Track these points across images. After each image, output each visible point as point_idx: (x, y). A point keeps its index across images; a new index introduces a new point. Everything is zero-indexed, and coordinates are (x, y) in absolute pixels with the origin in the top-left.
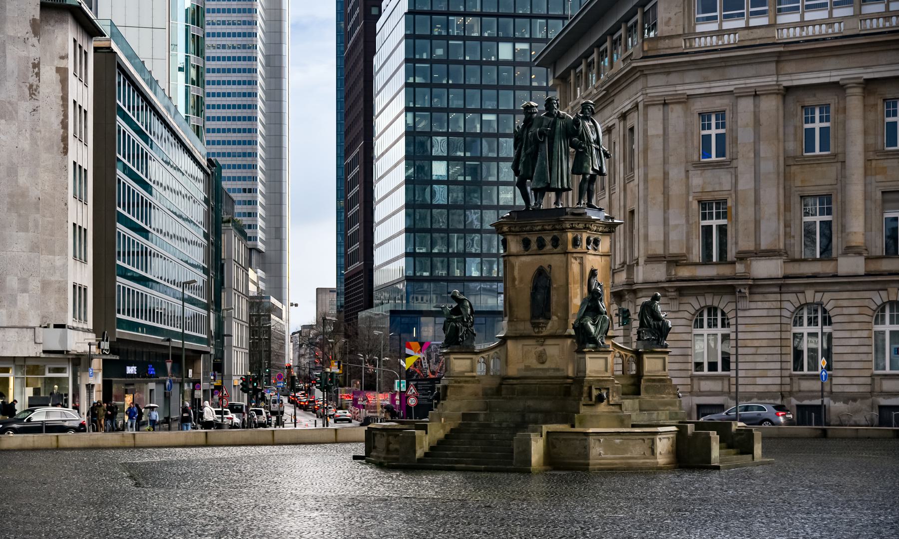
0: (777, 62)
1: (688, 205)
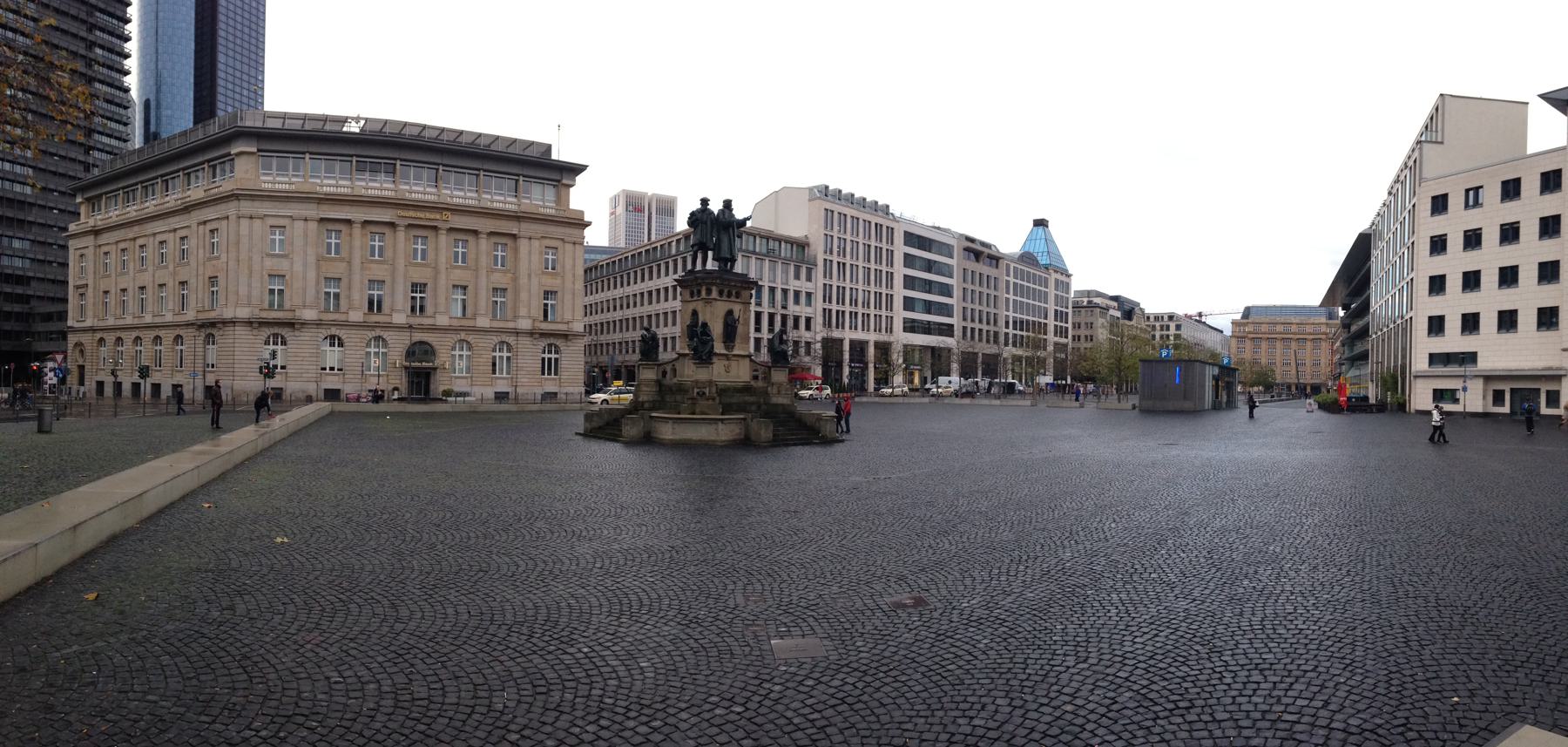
1: (262, 276)
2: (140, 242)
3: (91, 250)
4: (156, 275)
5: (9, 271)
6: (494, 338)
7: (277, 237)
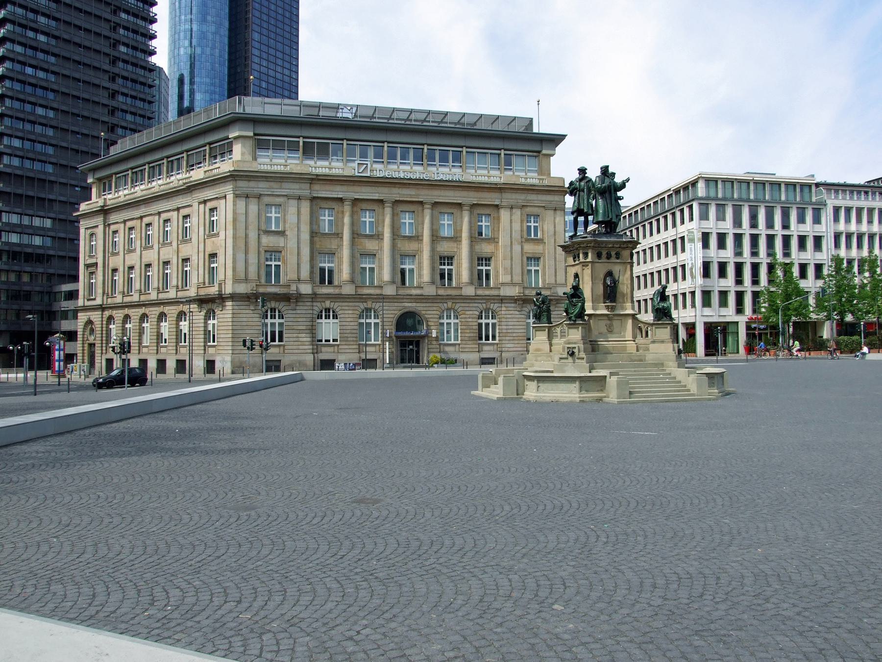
0: (311, 183)
2: (146, 220)
3: (101, 227)
4: (161, 252)
5: (29, 250)
6: (480, 305)
7: (273, 215)
